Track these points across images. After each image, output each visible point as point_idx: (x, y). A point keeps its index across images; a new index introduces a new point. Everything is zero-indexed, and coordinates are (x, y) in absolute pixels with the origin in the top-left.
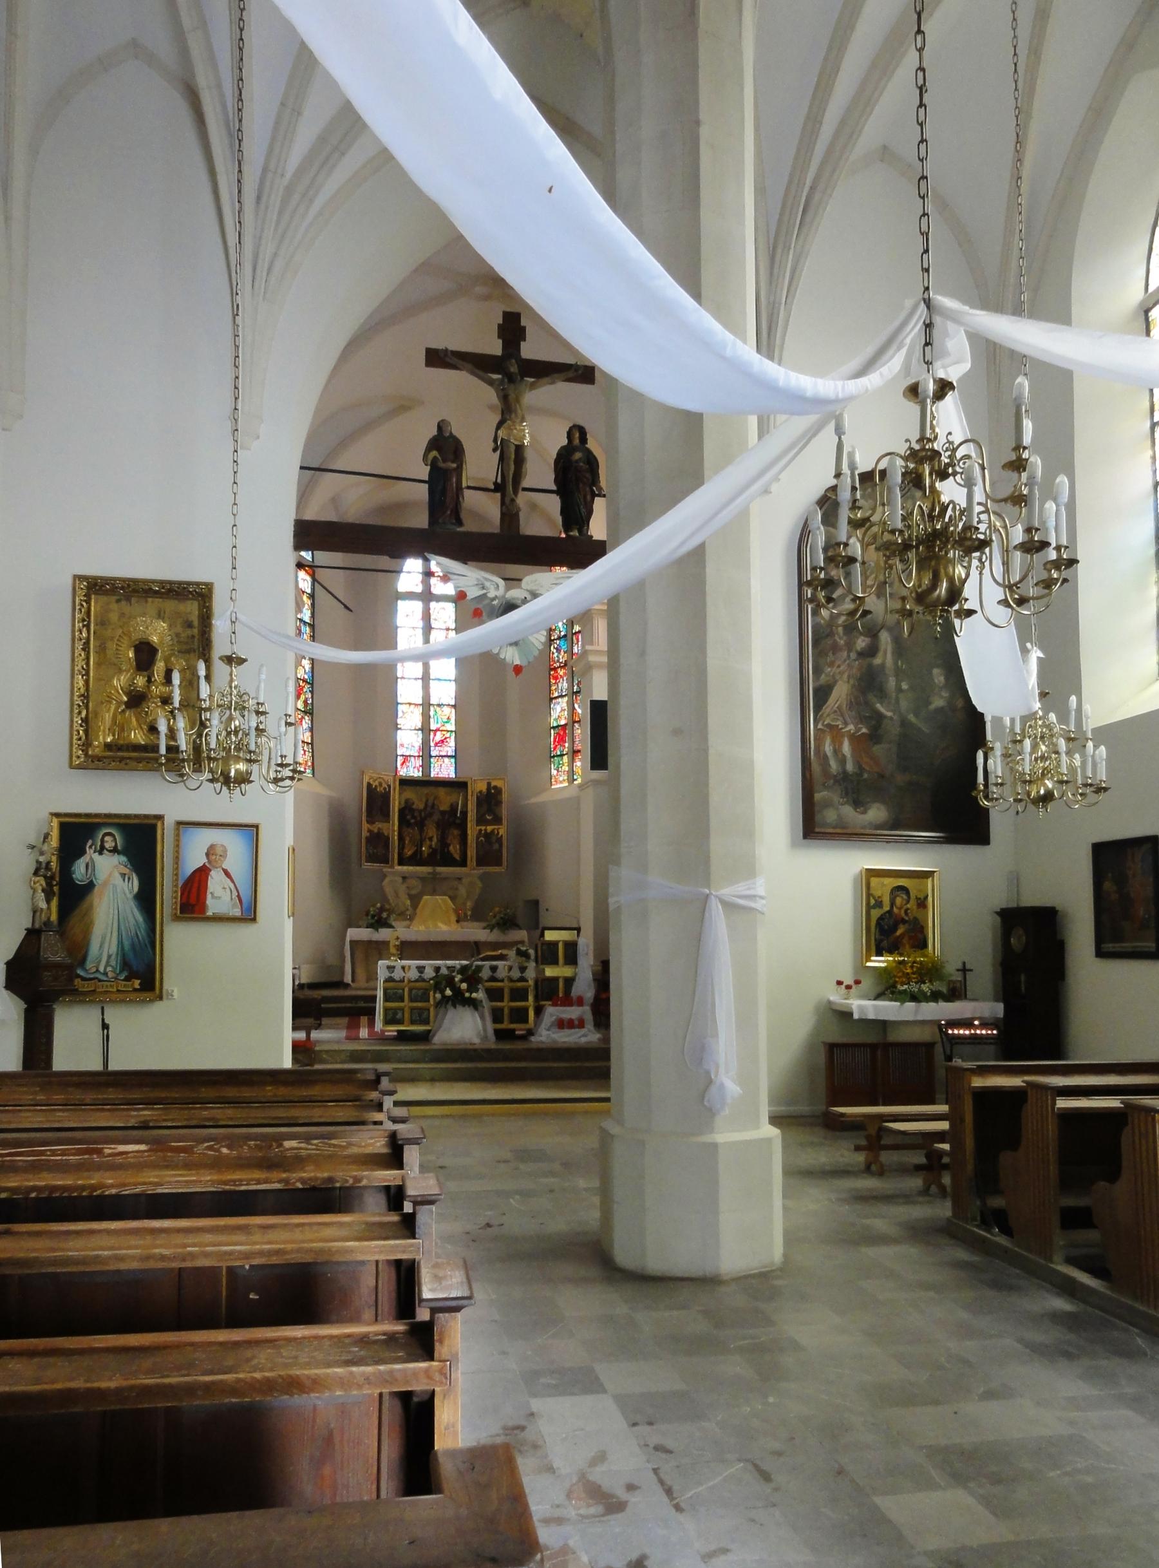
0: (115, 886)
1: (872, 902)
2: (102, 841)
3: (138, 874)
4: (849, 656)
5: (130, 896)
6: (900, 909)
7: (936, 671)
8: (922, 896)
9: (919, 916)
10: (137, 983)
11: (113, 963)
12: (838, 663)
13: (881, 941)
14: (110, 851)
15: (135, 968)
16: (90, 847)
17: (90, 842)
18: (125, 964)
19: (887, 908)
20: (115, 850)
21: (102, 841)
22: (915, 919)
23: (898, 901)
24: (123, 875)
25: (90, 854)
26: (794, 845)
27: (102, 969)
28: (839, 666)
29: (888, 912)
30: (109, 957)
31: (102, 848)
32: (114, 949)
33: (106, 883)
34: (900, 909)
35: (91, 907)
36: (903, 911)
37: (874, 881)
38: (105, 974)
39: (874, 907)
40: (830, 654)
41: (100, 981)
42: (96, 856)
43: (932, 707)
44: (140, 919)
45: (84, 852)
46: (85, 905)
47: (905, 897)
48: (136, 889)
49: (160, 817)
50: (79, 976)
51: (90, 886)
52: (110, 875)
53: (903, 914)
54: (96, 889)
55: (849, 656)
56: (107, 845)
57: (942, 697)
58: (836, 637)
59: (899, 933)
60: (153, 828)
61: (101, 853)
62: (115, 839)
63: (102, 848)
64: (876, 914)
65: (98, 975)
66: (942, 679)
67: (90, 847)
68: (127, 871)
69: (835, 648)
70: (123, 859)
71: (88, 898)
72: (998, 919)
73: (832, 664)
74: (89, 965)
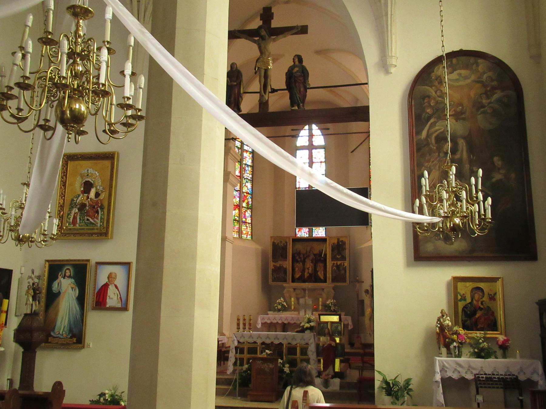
1: (459, 297)
2: (65, 272)
4: (439, 155)
5: (74, 298)
6: (478, 301)
7: (496, 159)
8: (492, 293)
9: (490, 306)
11: (66, 330)
12: (432, 160)
13: (466, 321)
19: (469, 300)
20: (70, 277)
21: (65, 272)
22: (488, 307)
23: (476, 296)
24: (72, 288)
26: (409, 265)
27: (61, 333)
28: (433, 161)
29: (470, 303)
32: (66, 323)
33: (65, 292)
34: (478, 301)
35: (58, 303)
36: (480, 303)
37: (460, 285)
38: (62, 335)
39: (460, 300)
40: (428, 155)
43: (494, 180)
44: (78, 309)
46: (56, 302)
47: (481, 294)
48: (77, 295)
49: (88, 261)
50: (51, 336)
51: (59, 293)
53: (480, 305)
55: (439, 155)
56: (67, 274)
57: (500, 174)
58: (431, 146)
59: (477, 316)
60: (86, 265)
61: (64, 278)
64: (461, 305)
65: (60, 336)
66: (500, 163)
69: (431, 152)
70: (73, 280)
72: (537, 307)
73: (428, 161)
74: (56, 330)
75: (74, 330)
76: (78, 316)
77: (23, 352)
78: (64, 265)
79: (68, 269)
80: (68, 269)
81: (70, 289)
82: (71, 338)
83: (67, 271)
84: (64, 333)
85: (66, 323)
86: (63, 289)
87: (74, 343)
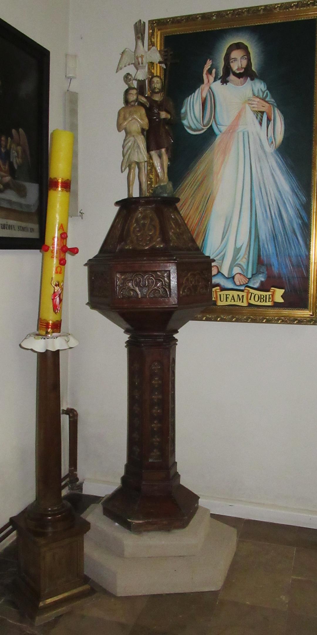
0: (246, 135)
2: (227, 59)
3: (283, 112)
5: (270, 149)
10: (278, 295)
11: (243, 262)
14: (239, 76)
15: (275, 270)
16: (210, 72)
17: (209, 64)
18: (261, 263)
20: (247, 74)
21: (227, 59)
25: (212, 85)
30: (237, 251)
31: (228, 70)
32: (243, 238)
33: (233, 128)
41: (223, 289)
42: (217, 86)
45: (201, 81)
46: (200, 167)
48: (280, 136)
51: (209, 135)
52: (239, 117)
54: (218, 140)
56: (235, 66)
61: (225, 81)
62: (248, 54)
63: (228, 70)
67: (210, 72)
68: (265, 107)
70: (260, 86)
71: (207, 156)
75: (274, 261)
76: (290, 212)
77: (129, 344)
78: (216, 36)
79: (239, 46)
80: (239, 46)
81: (250, 117)
82: (263, 288)
83: (236, 54)
84: (236, 270)
85: (242, 236)
86: (224, 119)
87: (276, 305)
